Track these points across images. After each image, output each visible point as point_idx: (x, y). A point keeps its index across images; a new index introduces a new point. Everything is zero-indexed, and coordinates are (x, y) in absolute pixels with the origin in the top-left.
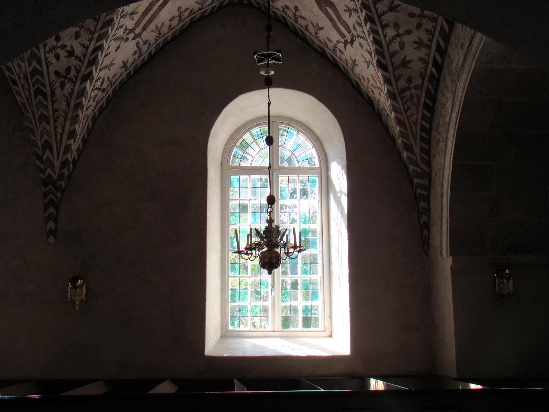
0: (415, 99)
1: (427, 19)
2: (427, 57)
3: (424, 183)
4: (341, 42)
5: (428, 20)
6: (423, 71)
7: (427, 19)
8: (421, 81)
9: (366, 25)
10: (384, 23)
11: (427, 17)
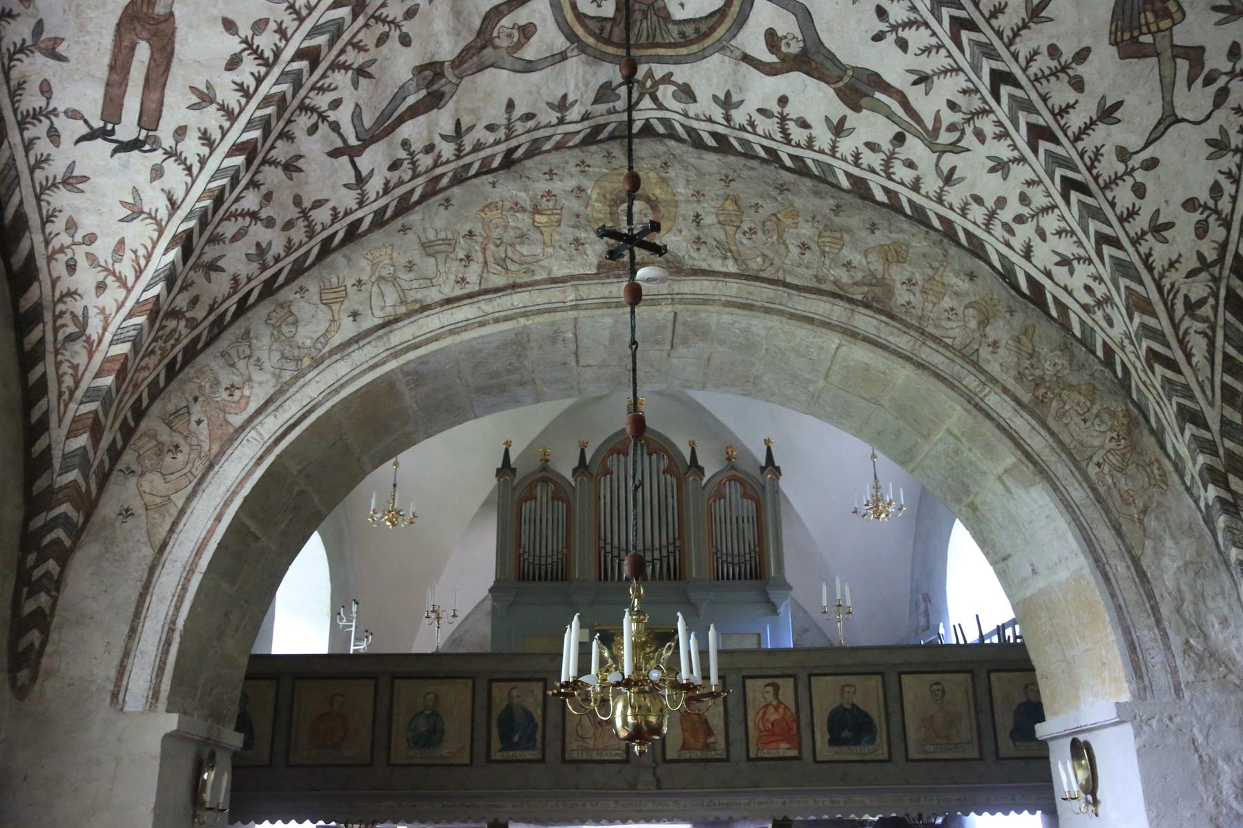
0: (172, 341)
1: (306, 223)
3: (75, 520)
4: (86, 122)
5: (305, 227)
6: (219, 300)
8: (205, 313)
9: (230, 154)
10: (259, 177)
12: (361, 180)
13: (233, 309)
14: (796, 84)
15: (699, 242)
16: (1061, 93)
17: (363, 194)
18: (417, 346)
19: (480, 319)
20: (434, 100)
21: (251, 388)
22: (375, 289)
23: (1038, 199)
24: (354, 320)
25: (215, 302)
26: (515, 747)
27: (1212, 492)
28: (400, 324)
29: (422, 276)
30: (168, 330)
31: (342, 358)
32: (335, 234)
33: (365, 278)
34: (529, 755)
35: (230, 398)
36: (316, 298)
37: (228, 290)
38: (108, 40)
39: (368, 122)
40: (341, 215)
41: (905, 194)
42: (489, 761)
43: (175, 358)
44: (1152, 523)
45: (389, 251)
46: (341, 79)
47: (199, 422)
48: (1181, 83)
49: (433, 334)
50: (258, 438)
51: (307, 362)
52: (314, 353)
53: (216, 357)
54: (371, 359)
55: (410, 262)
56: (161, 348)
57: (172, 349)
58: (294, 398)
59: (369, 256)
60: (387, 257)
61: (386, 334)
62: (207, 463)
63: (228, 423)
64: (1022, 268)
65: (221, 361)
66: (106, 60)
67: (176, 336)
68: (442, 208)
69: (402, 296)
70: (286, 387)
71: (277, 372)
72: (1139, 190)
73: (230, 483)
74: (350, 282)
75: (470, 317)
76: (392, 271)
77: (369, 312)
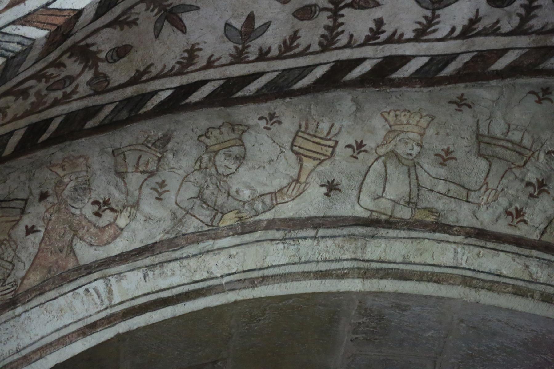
0: (59, 94)
1: (330, 23)
2: (204, 63)
5: (327, 28)
6: (154, 71)
7: (331, 24)
8: (124, 79)
11: (335, 20)
13: (164, 95)
17: (431, 21)
18: (403, 276)
19: (521, 283)
21: (132, 217)
22: (378, 166)
24: (327, 195)
25: (146, 71)
28: (392, 233)
29: (457, 180)
30: (64, 73)
31: (283, 240)
32: (360, 61)
33: (370, 144)
35: (94, 218)
36: (287, 139)
37: (173, 63)
40: (383, 37)
43: (49, 121)
45: (424, 123)
47: (30, 230)
49: (437, 270)
50: (104, 295)
51: (230, 220)
52: (246, 213)
53: (103, 151)
54: (325, 261)
55: (448, 152)
56: (38, 94)
57: (53, 105)
58: (185, 262)
59: (391, 118)
60: (417, 129)
61: (364, 236)
62: (9, 296)
63: (72, 251)
65: (108, 160)
67: (69, 90)
68: (535, 98)
69: (414, 195)
70: (183, 242)
71: (180, 213)
73: (27, 341)
74: (345, 139)
75: (504, 272)
76: (414, 153)
77: (355, 193)
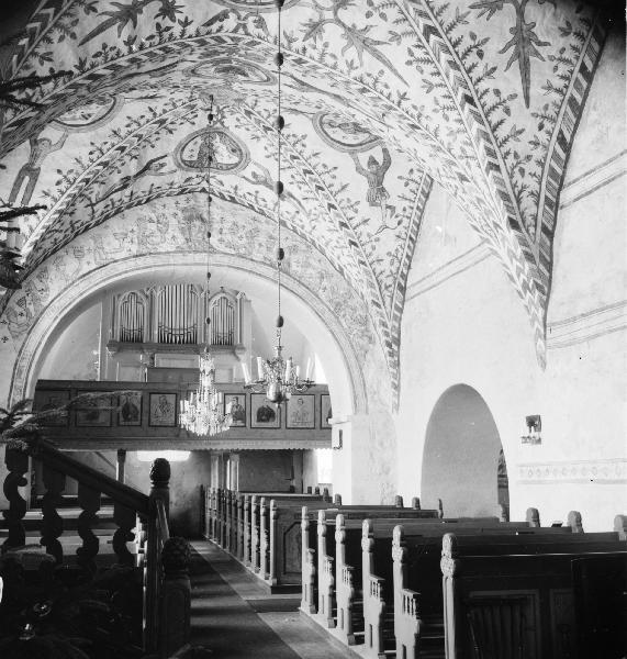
9: (55, 213)
12: (93, 212)
14: (261, 188)
15: (221, 241)
16: (350, 213)
20: (125, 187)
23: (342, 242)
26: (129, 420)
27: (387, 349)
34: (134, 423)
38: (15, 176)
39: (100, 196)
41: (298, 229)
42: (118, 425)
44: (368, 356)
46: (96, 185)
48: (388, 216)
64: (336, 262)
66: (13, 181)
72: (374, 248)
